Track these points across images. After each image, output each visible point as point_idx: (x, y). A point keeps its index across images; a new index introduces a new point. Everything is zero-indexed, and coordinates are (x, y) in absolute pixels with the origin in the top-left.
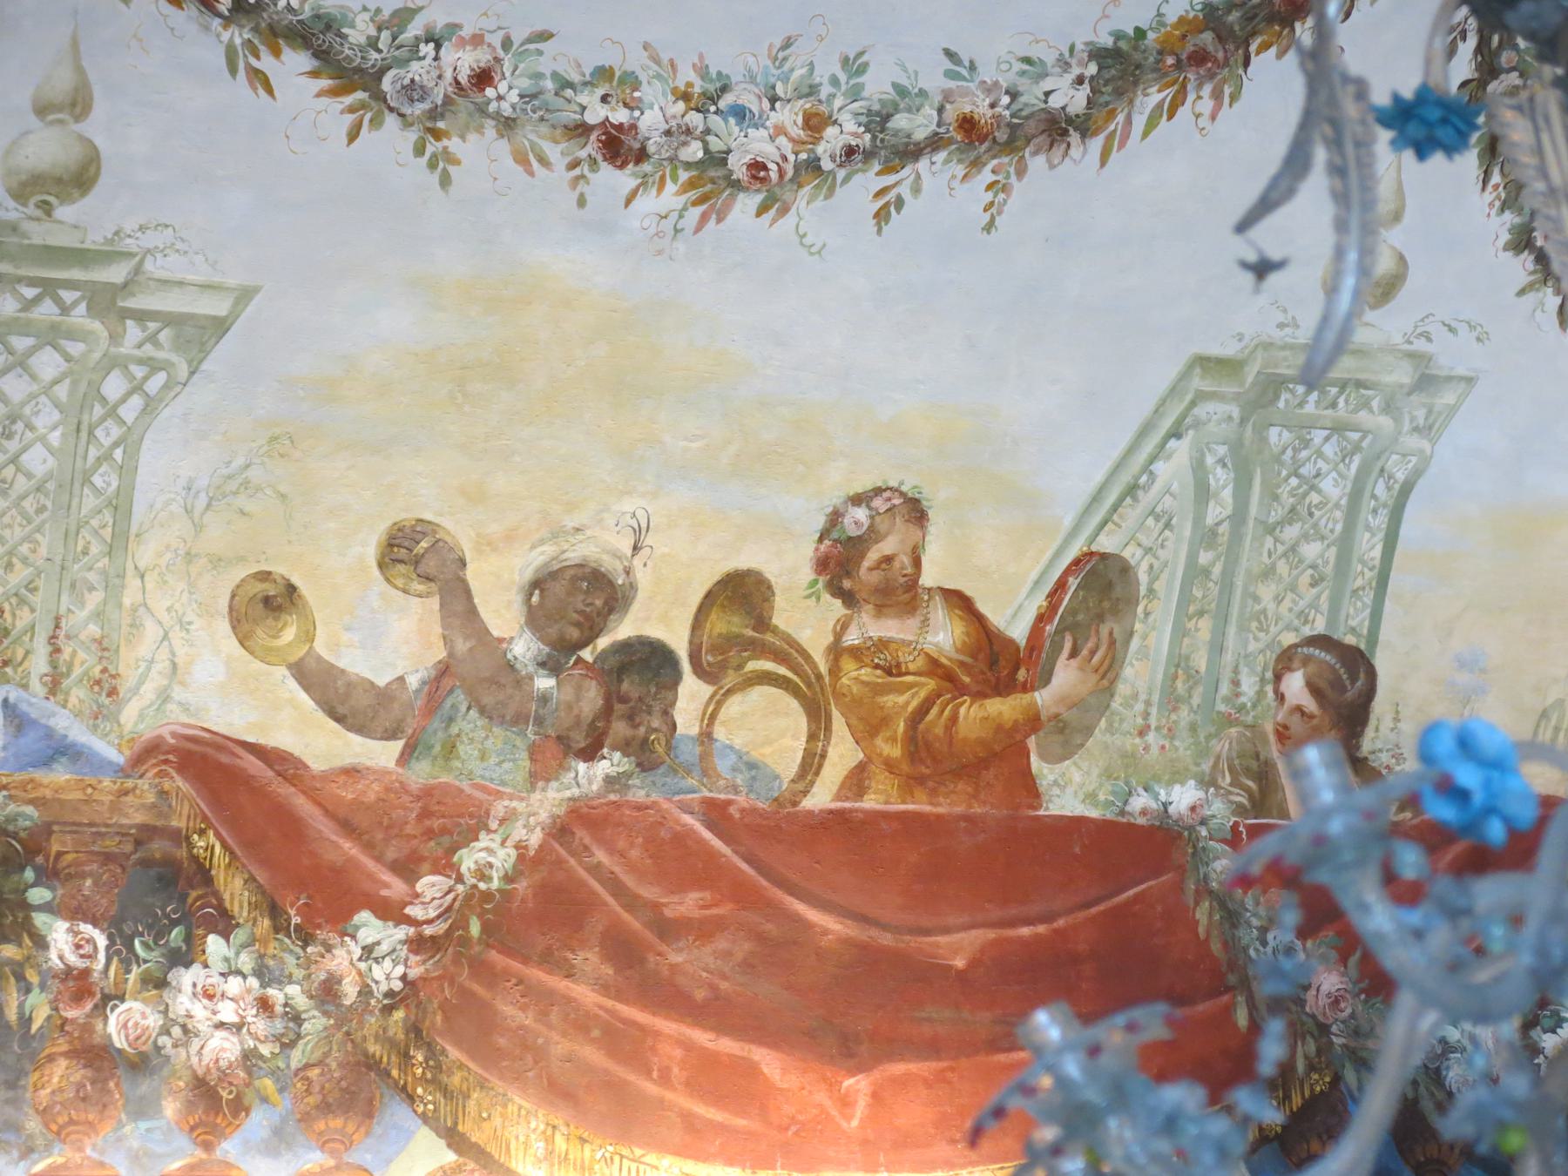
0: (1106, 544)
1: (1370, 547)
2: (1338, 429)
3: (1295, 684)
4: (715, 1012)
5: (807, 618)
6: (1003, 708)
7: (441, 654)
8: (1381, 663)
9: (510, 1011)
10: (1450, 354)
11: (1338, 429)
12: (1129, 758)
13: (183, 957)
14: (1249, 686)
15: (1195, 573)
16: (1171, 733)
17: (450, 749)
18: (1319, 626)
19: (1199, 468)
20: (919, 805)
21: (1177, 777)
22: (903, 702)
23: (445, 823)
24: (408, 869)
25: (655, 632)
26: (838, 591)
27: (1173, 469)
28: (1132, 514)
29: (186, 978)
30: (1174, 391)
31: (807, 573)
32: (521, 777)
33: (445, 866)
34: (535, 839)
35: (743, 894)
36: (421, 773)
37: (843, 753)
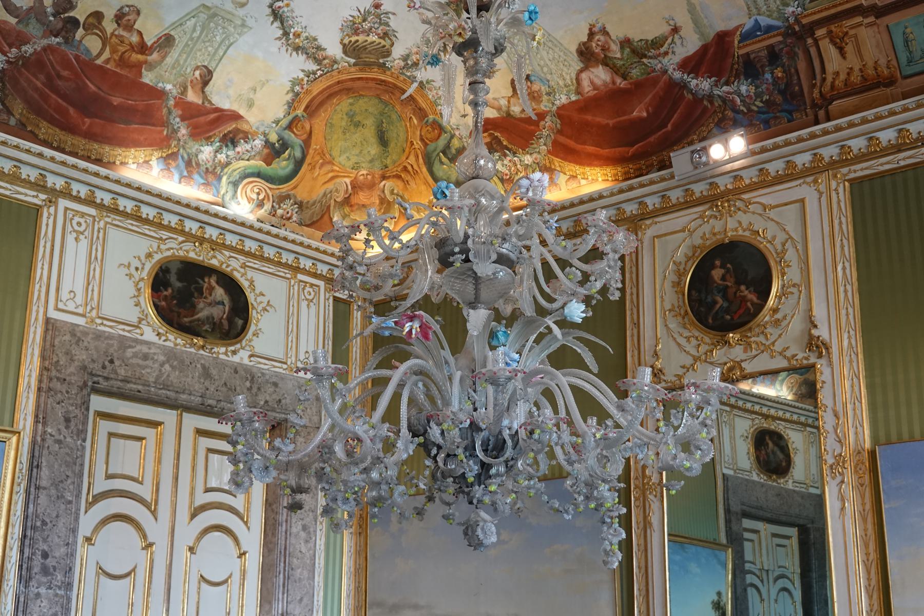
0: (172, 33)
1: (221, 53)
2: (224, 28)
3: (197, 73)
4: (64, 97)
5: (109, 26)
7: (32, 4)
8: (214, 75)
10: (250, 22)
11: (224, 28)
12: (161, 76)
14: (189, 70)
15: (187, 45)
16: (171, 74)
17: (27, 25)
18: (206, 64)
19: (195, 25)
20: (118, 70)
21: (169, 82)
22: (122, 49)
23: (21, 39)
24: (10, 46)
25: (78, 17)
26: (117, 22)
27: (190, 24)
28: (179, 29)
30: (196, 9)
31: (112, 17)
32: (40, 36)
33: (19, 48)
34: (39, 49)
36: (20, 27)
37: (106, 54)
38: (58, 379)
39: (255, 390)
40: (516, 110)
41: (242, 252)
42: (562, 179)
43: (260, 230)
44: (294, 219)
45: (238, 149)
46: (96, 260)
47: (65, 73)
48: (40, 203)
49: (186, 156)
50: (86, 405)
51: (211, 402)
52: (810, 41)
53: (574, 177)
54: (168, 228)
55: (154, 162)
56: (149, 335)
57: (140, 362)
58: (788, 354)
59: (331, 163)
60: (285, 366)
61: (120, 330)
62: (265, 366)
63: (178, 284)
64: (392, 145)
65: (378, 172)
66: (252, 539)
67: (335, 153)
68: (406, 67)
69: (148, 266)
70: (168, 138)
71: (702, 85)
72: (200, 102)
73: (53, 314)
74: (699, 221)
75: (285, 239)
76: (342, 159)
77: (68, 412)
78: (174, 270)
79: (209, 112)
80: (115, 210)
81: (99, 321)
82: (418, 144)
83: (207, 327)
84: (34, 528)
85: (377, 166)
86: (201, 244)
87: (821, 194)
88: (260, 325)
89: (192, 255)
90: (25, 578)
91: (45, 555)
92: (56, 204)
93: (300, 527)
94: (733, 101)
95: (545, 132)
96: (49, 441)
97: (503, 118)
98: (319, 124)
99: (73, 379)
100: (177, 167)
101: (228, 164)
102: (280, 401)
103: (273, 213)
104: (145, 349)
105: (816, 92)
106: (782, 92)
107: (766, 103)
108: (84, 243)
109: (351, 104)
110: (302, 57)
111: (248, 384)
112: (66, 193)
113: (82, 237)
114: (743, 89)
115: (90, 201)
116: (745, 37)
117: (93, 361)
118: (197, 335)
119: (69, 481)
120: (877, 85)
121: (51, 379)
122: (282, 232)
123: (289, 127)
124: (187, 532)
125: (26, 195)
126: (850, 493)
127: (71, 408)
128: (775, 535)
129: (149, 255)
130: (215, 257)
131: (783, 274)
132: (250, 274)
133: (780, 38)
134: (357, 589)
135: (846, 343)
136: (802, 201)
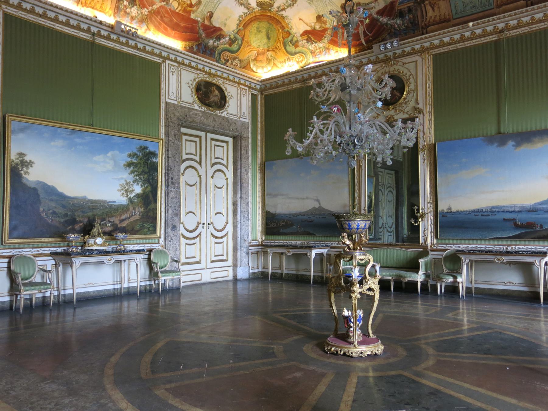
4: (166, 24)
6: (190, 9)
9: (153, 19)
13: (133, 7)
22: (185, 6)
24: (149, 6)
29: (133, 8)
35: (170, 15)
37: (180, 8)
40: (318, 27)
41: (222, 78)
42: (332, 52)
46: (178, 81)
52: (423, 5)
53: (337, 52)
54: (200, 70)
56: (196, 107)
58: (409, 113)
59: (250, 45)
61: (187, 105)
63: (204, 90)
64: (272, 39)
66: (229, 173)
67: (252, 42)
68: (279, 11)
71: (384, 20)
73: (168, 100)
74: (381, 68)
78: (202, 85)
80: (183, 64)
82: (281, 39)
83: (213, 104)
84: (168, 170)
85: (266, 47)
87: (423, 59)
89: (207, 79)
90: (167, 186)
91: (172, 179)
94: (394, 26)
95: (327, 35)
96: (170, 143)
97: (312, 30)
99: (176, 122)
104: (196, 112)
105: (423, 23)
106: (412, 23)
107: (406, 26)
108: (175, 76)
110: (243, 7)
112: (168, 58)
114: (398, 21)
115: (175, 61)
116: (400, 3)
118: (211, 107)
120: (444, 22)
121: (169, 122)
122: (236, 71)
123: (237, 33)
124: (211, 171)
126: (427, 157)
128: (388, 173)
129: (194, 80)
131: (409, 86)
132: (226, 85)
133: (412, 4)
134: (262, 190)
135: (428, 110)
136: (416, 61)
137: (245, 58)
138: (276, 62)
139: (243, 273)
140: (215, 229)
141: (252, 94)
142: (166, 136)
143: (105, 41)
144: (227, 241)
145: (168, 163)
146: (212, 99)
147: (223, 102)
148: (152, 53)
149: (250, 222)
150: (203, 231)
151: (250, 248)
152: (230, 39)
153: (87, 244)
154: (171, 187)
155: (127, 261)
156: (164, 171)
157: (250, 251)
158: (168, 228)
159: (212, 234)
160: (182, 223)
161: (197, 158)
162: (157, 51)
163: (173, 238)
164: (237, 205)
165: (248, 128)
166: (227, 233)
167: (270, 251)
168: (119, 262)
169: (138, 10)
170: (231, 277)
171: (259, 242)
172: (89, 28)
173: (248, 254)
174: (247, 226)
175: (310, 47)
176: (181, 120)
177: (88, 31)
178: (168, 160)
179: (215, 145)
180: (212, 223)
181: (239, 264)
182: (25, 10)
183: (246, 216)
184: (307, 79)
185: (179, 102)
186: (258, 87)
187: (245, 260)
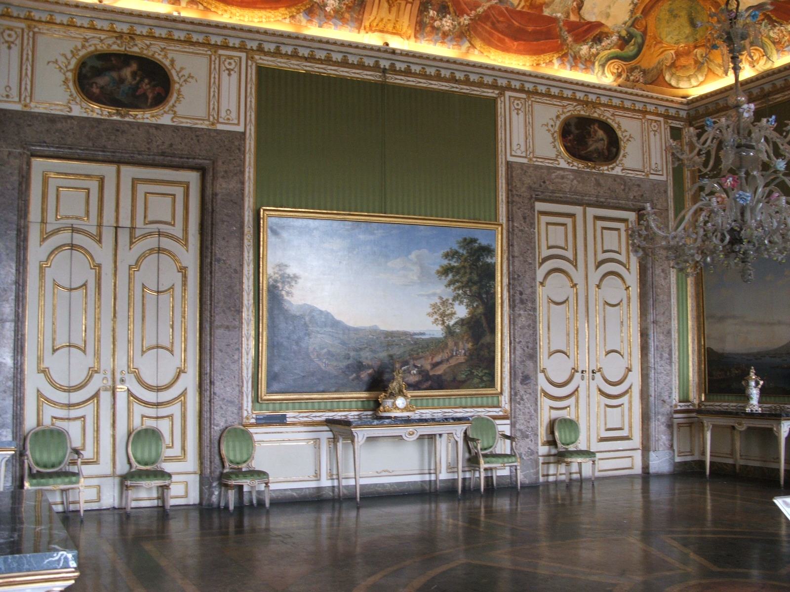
4: (502, 32)
9: (480, 29)
12: (554, 9)
13: (444, 17)
24: (471, 10)
29: (444, 19)
33: (475, 10)
37: (522, 4)
38: (517, 195)
39: (627, 190)
41: (611, 106)
43: (621, 92)
44: (641, 81)
45: (603, 44)
47: (501, 19)
48: (495, 96)
49: (572, 53)
50: (533, 208)
51: (602, 200)
55: (555, 61)
56: (563, 164)
57: (560, 180)
59: (661, 42)
60: (644, 174)
61: (547, 163)
62: (631, 174)
63: (577, 132)
65: (692, 44)
67: (663, 36)
69: (558, 123)
70: (562, 45)
72: (578, 20)
73: (510, 159)
75: (637, 95)
76: (668, 39)
77: (524, 213)
79: (583, 25)
80: (536, 93)
81: (534, 159)
84: (514, 279)
86: (587, 106)
88: (626, 150)
89: (582, 113)
90: (512, 306)
91: (521, 293)
92: (504, 95)
93: (660, 271)
96: (516, 231)
98: (651, 21)
99: (525, 194)
100: (569, 61)
101: (598, 54)
102: (642, 195)
103: (627, 79)
108: (522, 115)
109: (670, 4)
111: (622, 187)
112: (509, 88)
113: (520, 112)
115: (522, 90)
117: (535, 183)
118: (590, 160)
119: (529, 252)
121: (513, 196)
122: (635, 91)
123: (633, 25)
124: (595, 276)
125: (488, 92)
127: (526, 211)
129: (558, 117)
130: (595, 112)
132: (617, 119)
134: (698, 306)
137: (652, 65)
138: (712, 66)
139: (660, 462)
140: (606, 381)
141: (672, 128)
142: (508, 220)
143: (402, 78)
144: (630, 402)
145: (513, 266)
146: (593, 146)
147: (614, 150)
148: (481, 84)
149: (675, 367)
150: (583, 385)
151: (676, 416)
152: (621, 37)
153: (381, 408)
154: (520, 309)
155: (445, 436)
156: (506, 281)
157: (676, 421)
158: (515, 379)
159: (600, 390)
160: (543, 371)
161: (569, 254)
162: (488, 80)
163: (525, 397)
164: (647, 335)
165: (666, 192)
166: (630, 388)
167: (708, 423)
168: (432, 437)
169: (453, 20)
170: (638, 470)
171: (693, 405)
172: (377, 62)
173: (670, 426)
174: (669, 374)
175: (771, 34)
176: (535, 189)
177: (376, 67)
178: (513, 262)
179: (604, 228)
180: (599, 370)
181: (653, 444)
182: (286, 55)
183: (666, 355)
184: (769, 94)
185: (530, 159)
186: (683, 114)
187: (664, 438)
